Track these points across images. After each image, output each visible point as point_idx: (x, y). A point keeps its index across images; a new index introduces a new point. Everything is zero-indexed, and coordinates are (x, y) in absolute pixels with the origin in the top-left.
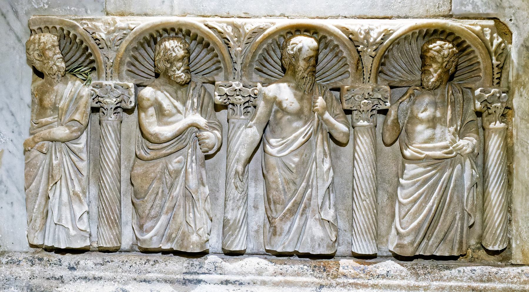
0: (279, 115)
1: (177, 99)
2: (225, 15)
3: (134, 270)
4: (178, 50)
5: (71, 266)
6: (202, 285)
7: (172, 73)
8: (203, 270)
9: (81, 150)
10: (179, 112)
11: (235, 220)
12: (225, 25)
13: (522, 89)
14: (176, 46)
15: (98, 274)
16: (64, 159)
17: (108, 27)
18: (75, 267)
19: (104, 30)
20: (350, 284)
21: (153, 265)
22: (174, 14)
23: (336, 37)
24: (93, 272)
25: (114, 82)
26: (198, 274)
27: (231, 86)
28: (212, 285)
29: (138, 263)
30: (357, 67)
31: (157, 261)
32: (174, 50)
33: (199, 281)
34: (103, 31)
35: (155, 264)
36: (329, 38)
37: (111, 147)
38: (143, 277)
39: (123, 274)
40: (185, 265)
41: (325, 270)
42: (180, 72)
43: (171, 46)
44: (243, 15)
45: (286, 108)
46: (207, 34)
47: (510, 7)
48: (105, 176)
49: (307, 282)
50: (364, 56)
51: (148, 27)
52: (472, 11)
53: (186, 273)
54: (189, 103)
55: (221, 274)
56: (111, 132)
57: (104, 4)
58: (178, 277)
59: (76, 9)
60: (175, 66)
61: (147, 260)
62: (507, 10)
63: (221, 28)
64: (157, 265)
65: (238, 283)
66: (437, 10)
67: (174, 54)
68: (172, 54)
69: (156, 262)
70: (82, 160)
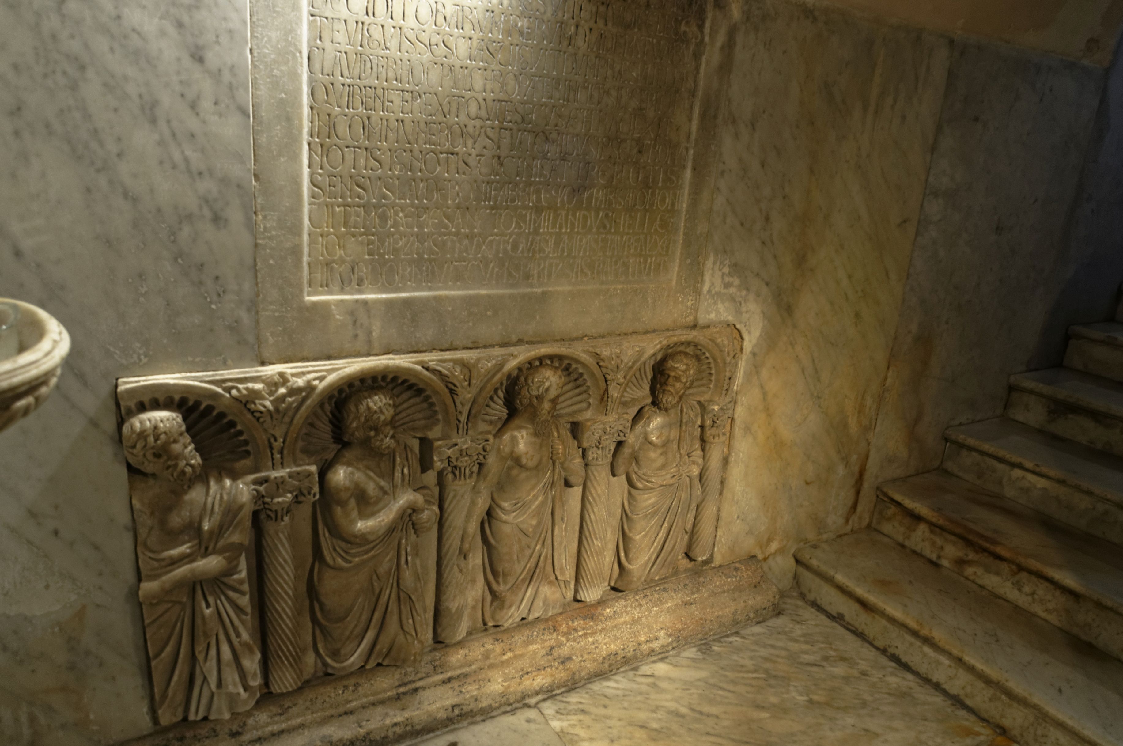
0: (515, 472)
1: (382, 476)
2: (446, 346)
3: (328, 705)
4: (387, 410)
5: (234, 731)
6: (421, 693)
7: (378, 443)
8: (419, 676)
9: (241, 582)
10: (385, 493)
11: (458, 607)
12: (451, 364)
13: (743, 398)
14: (385, 405)
15: (276, 728)
16: (219, 602)
17: (274, 389)
18: (240, 730)
19: (268, 394)
20: (580, 636)
21: (353, 691)
22: (374, 352)
23: (584, 365)
24: (270, 728)
25: (288, 470)
26: (414, 682)
27: (456, 445)
28: (432, 689)
29: (333, 695)
30: (602, 399)
31: (358, 683)
32: (381, 412)
33: (416, 690)
34: (267, 396)
35: (356, 689)
36: (574, 366)
37: (285, 561)
38: (341, 710)
39: (315, 715)
40: (397, 676)
41: (555, 630)
42: (388, 439)
43: (378, 406)
44: (470, 345)
45: (525, 464)
46: (429, 381)
47: (747, 312)
48: (278, 602)
49: (538, 649)
50: (611, 385)
51: (341, 383)
52: (714, 319)
53: (400, 686)
54: (398, 475)
55: (441, 673)
56: (284, 540)
57: (256, 347)
58: (389, 694)
59: (204, 359)
60: (382, 433)
61: (344, 687)
62: (744, 315)
63: (447, 370)
64: (360, 689)
65: (462, 676)
66: (684, 320)
67: (382, 418)
68: (379, 418)
69: (357, 685)
70: (243, 593)
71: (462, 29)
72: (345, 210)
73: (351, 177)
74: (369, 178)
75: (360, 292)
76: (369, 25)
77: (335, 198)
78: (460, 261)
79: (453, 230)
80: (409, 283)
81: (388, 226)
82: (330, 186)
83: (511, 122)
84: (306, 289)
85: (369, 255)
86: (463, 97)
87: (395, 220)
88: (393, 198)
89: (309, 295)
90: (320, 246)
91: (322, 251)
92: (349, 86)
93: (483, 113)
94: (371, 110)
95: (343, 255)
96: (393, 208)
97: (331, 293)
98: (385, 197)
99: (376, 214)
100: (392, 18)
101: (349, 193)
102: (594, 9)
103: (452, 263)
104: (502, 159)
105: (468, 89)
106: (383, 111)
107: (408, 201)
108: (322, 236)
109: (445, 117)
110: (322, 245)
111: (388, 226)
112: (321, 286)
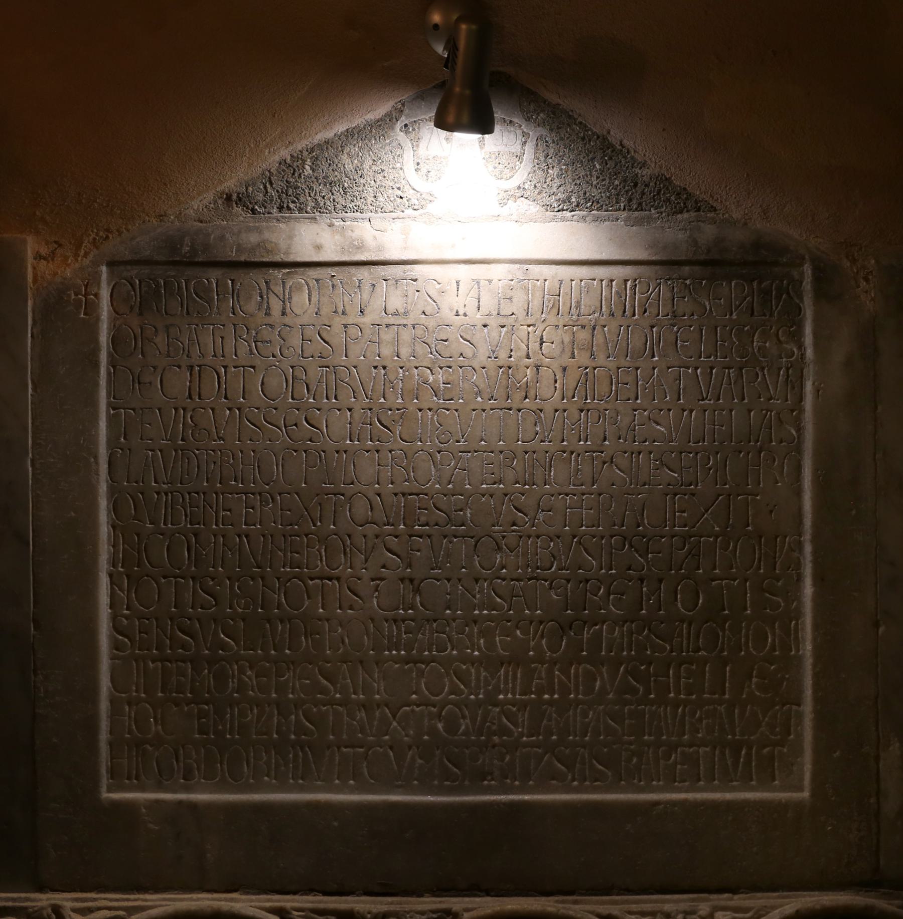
71: (336, 398)
72: (163, 666)
73: (171, 619)
74: (198, 620)
75: (187, 789)
76: (194, 410)
77: (148, 650)
78: (353, 747)
79: (338, 696)
80: (266, 778)
81: (230, 690)
82: (140, 632)
83: (427, 525)
84: (105, 781)
85: (200, 733)
86: (343, 495)
87: (240, 680)
88: (236, 648)
89: (109, 791)
90: (127, 718)
91: (130, 725)
92: (166, 494)
93: (381, 517)
94: (199, 524)
95: (162, 733)
96: (237, 663)
97: (143, 789)
98: (224, 646)
99: (209, 672)
100: (226, 398)
101: (168, 641)
102: (567, 339)
103: (339, 748)
104: (416, 582)
105: (350, 482)
106: (216, 525)
107: (259, 652)
108: (129, 704)
109: (314, 525)
110: (130, 717)
111: (230, 690)
112: (129, 778)
